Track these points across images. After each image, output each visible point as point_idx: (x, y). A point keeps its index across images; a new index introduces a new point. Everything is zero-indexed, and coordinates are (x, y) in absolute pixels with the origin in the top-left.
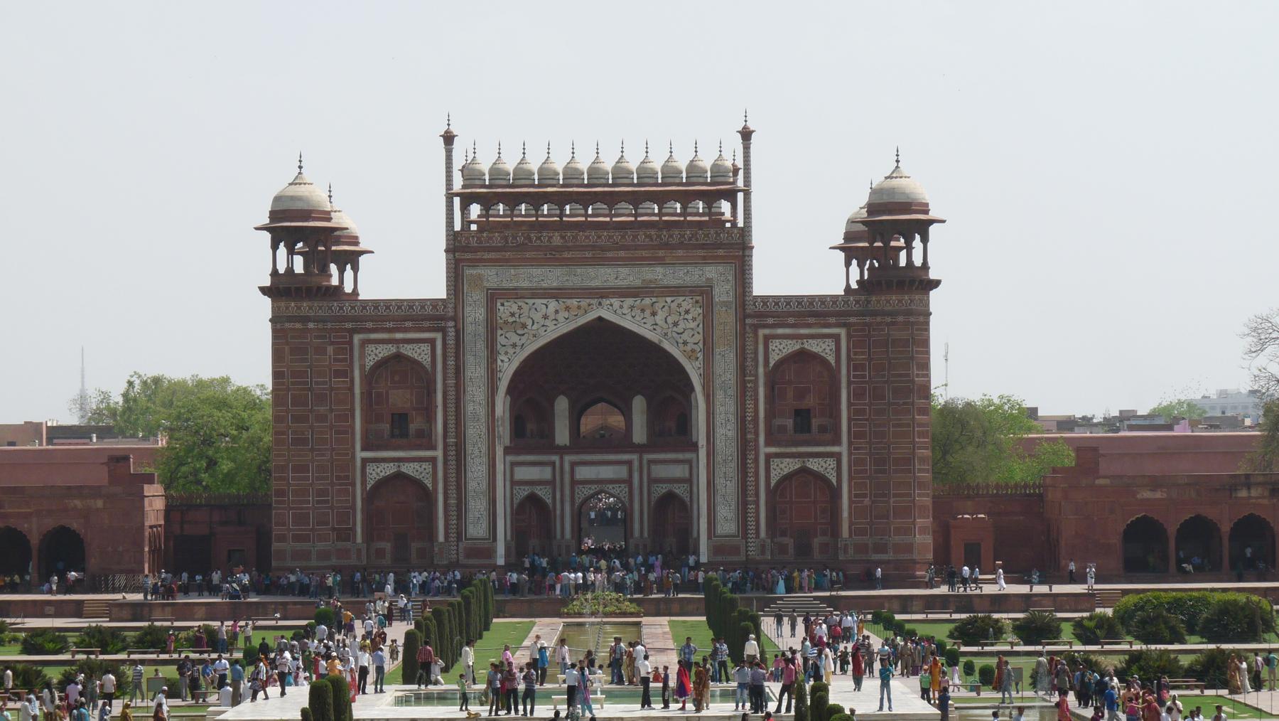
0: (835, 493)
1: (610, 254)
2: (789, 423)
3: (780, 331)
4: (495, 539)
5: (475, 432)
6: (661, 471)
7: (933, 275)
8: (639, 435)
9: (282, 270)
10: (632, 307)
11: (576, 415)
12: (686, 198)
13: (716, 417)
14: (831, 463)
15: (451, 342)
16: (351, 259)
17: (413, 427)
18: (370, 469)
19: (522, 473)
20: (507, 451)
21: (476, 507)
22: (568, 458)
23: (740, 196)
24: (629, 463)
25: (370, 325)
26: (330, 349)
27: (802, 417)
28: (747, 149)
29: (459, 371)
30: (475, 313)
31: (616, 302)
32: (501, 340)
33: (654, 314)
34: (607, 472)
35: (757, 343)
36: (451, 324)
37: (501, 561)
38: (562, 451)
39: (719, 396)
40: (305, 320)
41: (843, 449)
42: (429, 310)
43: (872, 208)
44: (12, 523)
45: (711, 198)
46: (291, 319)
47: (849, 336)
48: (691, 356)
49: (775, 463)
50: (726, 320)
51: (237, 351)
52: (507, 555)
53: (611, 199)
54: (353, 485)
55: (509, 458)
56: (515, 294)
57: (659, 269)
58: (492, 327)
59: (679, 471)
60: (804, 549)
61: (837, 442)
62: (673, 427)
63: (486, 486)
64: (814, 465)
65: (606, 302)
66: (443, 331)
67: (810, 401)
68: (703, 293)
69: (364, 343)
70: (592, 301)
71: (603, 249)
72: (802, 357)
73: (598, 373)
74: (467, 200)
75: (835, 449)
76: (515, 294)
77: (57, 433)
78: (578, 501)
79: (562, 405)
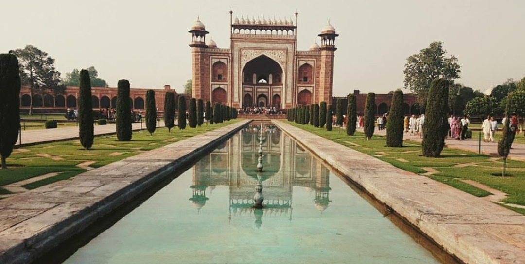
1: (265, 40)
2: (303, 79)
3: (302, 59)
4: (239, 102)
5: (236, 79)
6: (274, 90)
7: (335, 47)
8: (271, 82)
9: (194, 40)
10: (270, 52)
13: (288, 77)
14: (312, 88)
15: (231, 58)
17: (223, 78)
18: (213, 86)
19: (246, 89)
20: (243, 84)
21: (236, 95)
22: (256, 87)
23: (294, 29)
24: (268, 88)
25: (213, 54)
26: (205, 59)
28: (297, 17)
29: (232, 65)
30: (236, 53)
31: (267, 51)
32: (242, 59)
33: (275, 54)
34: (264, 90)
35: (296, 61)
36: (230, 55)
37: (241, 107)
38: (254, 85)
39: (288, 73)
40: (199, 52)
41: (314, 85)
42: (226, 52)
44: (140, 96)
46: (195, 52)
47: (317, 61)
48: (282, 64)
49: (300, 87)
52: (242, 105)
54: (210, 89)
55: (244, 86)
56: (245, 49)
57: (276, 44)
58: (240, 56)
59: (279, 90)
61: (313, 83)
62: (278, 80)
64: (308, 88)
65: (265, 51)
66: (229, 56)
67: (307, 75)
68: (286, 50)
69: (212, 58)
70: (262, 51)
71: (265, 39)
72: (306, 65)
74: (235, 26)
75: (312, 85)
76: (245, 49)
78: (257, 96)
79: (255, 75)
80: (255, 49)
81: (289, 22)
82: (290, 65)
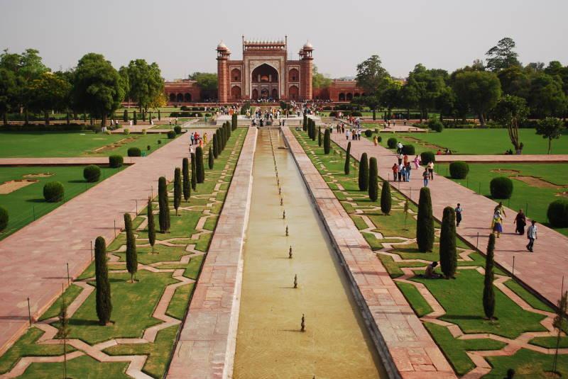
0: (298, 89)
5: (247, 80)
8: (270, 80)
11: (261, 77)
12: (277, 46)
13: (281, 76)
16: (228, 54)
21: (247, 91)
27: (294, 78)
30: (246, 63)
43: (305, 48)
45: (280, 46)
50: (282, 64)
51: (213, 69)
53: (267, 46)
56: (252, 60)
58: (249, 64)
60: (294, 97)
62: (275, 79)
63: (249, 88)
67: (295, 76)
68: (279, 60)
72: (294, 69)
73: (265, 72)
76: (252, 60)
77: (184, 80)
79: (259, 76)
80: (259, 60)
81: (280, 40)
82: (283, 72)
